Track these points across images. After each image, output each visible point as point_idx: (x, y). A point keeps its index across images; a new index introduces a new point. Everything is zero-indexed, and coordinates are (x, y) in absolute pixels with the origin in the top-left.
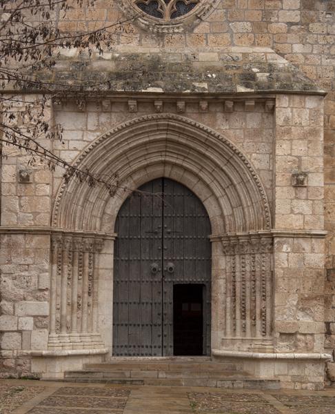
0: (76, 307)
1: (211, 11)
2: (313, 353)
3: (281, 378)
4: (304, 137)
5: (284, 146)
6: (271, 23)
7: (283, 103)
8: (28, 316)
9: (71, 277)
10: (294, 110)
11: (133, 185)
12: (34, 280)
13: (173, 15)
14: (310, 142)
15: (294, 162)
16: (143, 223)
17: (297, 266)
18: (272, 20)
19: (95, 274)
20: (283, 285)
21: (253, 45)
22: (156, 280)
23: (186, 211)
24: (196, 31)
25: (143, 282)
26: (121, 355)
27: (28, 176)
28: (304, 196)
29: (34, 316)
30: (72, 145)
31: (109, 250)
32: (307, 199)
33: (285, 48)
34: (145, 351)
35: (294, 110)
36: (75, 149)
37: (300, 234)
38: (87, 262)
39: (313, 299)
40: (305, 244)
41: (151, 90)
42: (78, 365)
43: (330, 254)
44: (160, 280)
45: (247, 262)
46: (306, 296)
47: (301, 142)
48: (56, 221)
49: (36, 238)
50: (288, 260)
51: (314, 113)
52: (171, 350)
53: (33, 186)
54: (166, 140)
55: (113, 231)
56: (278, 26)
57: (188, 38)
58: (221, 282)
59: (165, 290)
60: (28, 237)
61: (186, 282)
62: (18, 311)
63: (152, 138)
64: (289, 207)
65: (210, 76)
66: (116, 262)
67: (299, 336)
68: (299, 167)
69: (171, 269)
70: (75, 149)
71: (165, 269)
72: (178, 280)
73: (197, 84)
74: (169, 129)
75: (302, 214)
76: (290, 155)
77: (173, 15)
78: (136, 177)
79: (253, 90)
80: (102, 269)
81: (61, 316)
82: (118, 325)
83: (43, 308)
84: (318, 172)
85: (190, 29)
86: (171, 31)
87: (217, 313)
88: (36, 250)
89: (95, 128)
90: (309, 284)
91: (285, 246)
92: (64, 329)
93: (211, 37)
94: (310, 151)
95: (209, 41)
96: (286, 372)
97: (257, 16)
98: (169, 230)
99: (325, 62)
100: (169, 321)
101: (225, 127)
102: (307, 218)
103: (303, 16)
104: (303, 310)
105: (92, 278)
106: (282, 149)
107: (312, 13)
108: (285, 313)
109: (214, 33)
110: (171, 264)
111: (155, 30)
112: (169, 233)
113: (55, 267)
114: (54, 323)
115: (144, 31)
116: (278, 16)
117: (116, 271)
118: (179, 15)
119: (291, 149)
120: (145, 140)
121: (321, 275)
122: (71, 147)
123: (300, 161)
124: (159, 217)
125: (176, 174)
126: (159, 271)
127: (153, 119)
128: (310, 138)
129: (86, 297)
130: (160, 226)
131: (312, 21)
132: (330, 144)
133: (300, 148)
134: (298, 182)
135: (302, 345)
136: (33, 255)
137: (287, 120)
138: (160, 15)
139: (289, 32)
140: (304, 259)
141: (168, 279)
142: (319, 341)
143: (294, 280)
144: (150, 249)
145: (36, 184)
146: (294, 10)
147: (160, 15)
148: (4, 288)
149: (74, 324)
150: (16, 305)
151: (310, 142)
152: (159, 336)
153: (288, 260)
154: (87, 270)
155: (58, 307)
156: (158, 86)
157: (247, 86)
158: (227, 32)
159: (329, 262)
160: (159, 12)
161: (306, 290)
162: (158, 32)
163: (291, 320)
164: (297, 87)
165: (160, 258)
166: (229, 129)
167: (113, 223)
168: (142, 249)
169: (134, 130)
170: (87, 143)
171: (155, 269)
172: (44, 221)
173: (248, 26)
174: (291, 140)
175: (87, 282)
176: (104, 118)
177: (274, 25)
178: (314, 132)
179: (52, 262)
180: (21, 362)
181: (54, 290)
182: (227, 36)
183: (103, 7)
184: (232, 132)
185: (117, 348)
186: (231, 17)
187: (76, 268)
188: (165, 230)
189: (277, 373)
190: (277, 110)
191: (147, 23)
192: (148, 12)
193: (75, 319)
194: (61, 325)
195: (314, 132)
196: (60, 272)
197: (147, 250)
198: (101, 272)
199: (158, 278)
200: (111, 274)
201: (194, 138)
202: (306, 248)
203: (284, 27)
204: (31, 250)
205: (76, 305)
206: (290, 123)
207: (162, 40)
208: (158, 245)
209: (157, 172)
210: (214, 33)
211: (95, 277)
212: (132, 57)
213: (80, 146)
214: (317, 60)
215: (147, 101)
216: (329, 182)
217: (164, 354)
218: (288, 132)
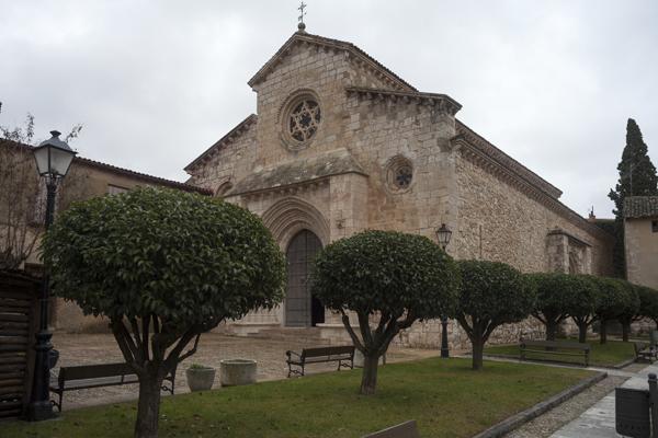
7: (333, 180)
33: (351, 146)
42: (256, 330)
78: (290, 230)
97: (338, 130)
100: (309, 307)
101: (313, 198)
106: (333, 207)
125: (307, 227)
131: (365, 126)
133: (341, 205)
137: (335, 191)
139: (355, 134)
164: (340, 170)
169: (277, 206)
173: (334, 137)
176: (265, 203)
178: (348, 195)
195: (348, 195)
201: (302, 206)
203: (351, 133)
215: (277, 191)
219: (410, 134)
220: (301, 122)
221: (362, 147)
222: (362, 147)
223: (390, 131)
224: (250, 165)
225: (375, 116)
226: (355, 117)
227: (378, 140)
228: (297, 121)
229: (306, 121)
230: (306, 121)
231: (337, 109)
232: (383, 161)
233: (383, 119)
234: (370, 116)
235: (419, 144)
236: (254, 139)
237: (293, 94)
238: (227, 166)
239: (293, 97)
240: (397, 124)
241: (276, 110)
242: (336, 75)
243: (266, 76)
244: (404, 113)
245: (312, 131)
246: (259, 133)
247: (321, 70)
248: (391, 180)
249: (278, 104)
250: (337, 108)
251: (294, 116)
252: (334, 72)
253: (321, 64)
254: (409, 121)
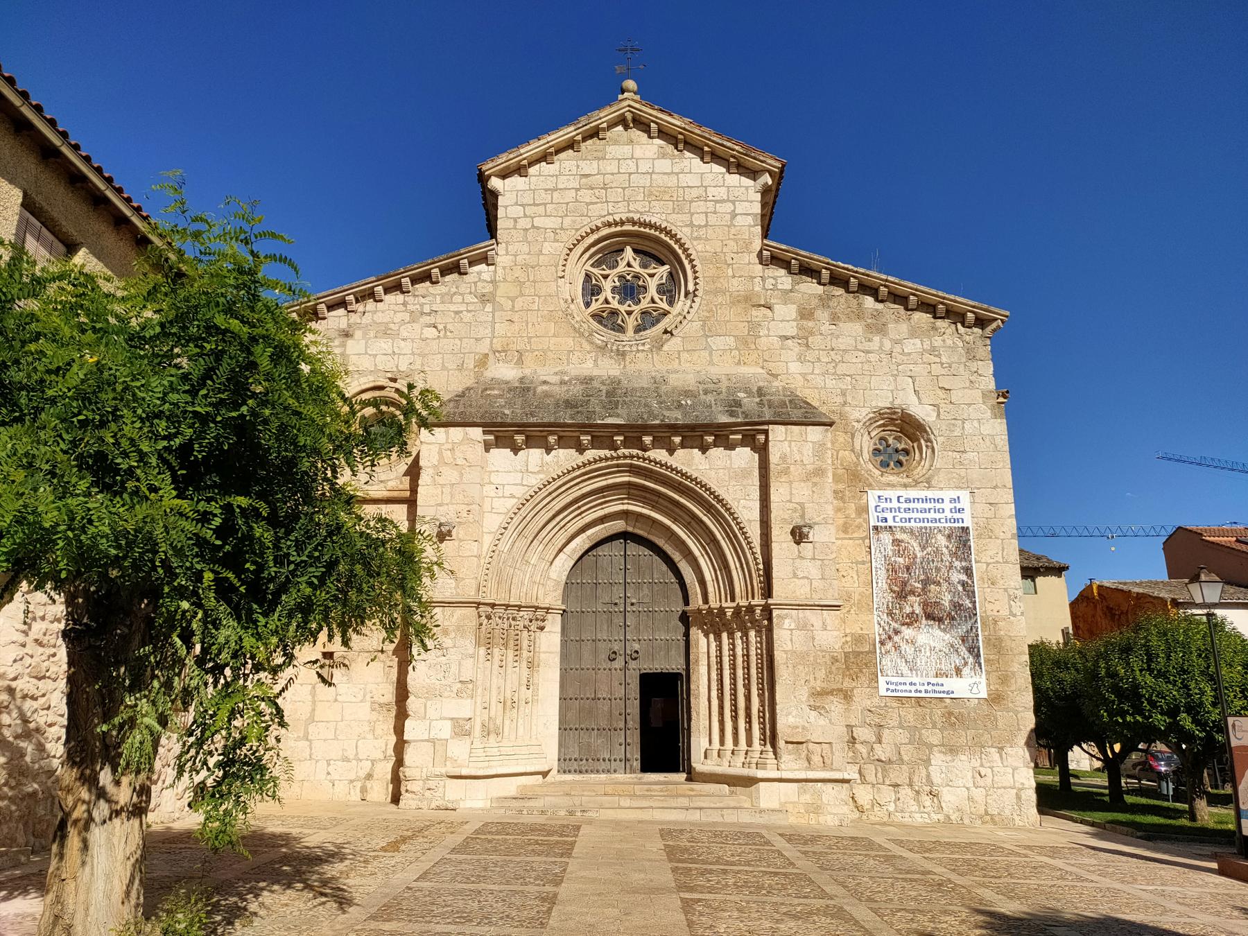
0: (510, 704)
1: (685, 322)
2: (832, 770)
3: (790, 807)
4: (807, 478)
5: (781, 490)
6: (760, 337)
8: (446, 719)
9: (504, 663)
10: (793, 443)
11: (587, 541)
12: (454, 668)
13: (638, 329)
14: (815, 484)
15: (795, 510)
16: (599, 591)
17: (806, 649)
18: (761, 334)
19: (536, 659)
20: (786, 675)
21: (739, 363)
23: (655, 576)
24: (665, 348)
26: (570, 772)
27: (450, 531)
28: (809, 554)
29: (452, 719)
30: (508, 490)
31: (554, 625)
32: (814, 559)
34: (603, 766)
35: (793, 443)
36: (512, 496)
37: (807, 605)
38: (525, 644)
39: (827, 694)
40: (813, 617)
41: (609, 421)
43: (848, 631)
45: (739, 642)
46: (819, 689)
47: (803, 484)
48: (484, 589)
49: (459, 612)
50: (791, 640)
51: (820, 449)
52: (637, 764)
53: (456, 543)
54: (629, 484)
55: (560, 602)
56: (768, 341)
57: (655, 355)
58: (703, 669)
59: (628, 680)
60: (448, 611)
62: (431, 713)
63: (610, 481)
64: (790, 569)
65: (683, 402)
66: (564, 643)
67: (811, 746)
68: (802, 516)
70: (512, 496)
71: (628, 652)
73: (667, 413)
74: (634, 470)
75: (808, 578)
76: (791, 502)
77: (638, 329)
79: (739, 420)
80: (544, 652)
81: (490, 718)
82: (565, 730)
83: (463, 709)
84: (826, 523)
85: (658, 345)
86: (634, 348)
87: (698, 714)
88: (459, 629)
89: (538, 469)
90: (821, 674)
91: (787, 621)
92: (492, 736)
93: (685, 356)
94: (815, 495)
95: (682, 361)
96: (796, 800)
97: (743, 329)
98: (634, 601)
99: (830, 383)
102: (815, 584)
103: (800, 328)
104: (813, 708)
105: (531, 665)
107: (811, 324)
108: (790, 714)
109: (688, 351)
110: (636, 646)
111: (614, 348)
112: (632, 604)
113: (482, 651)
114: (478, 728)
115: (603, 348)
116: (769, 330)
117: (565, 656)
118: (645, 329)
119: (791, 494)
120: (604, 483)
121: (837, 661)
122: (507, 494)
123: (803, 509)
127: (612, 458)
128: (815, 480)
129: (525, 694)
131: (812, 333)
132: (841, 486)
133: (802, 492)
134: (799, 535)
135: (816, 759)
136: (453, 635)
137: (783, 458)
138: (621, 329)
140: (814, 639)
142: (840, 754)
143: (801, 668)
145: (461, 540)
146: (788, 321)
147: (621, 329)
148: (414, 680)
149: (506, 730)
150: (429, 703)
151: (815, 484)
152: (620, 745)
153: (791, 640)
154: (525, 654)
155: (486, 705)
156: (618, 416)
157: (731, 416)
158: (705, 348)
159: (847, 642)
160: (619, 325)
161: (818, 682)
162: (618, 350)
163: (800, 722)
165: (622, 638)
166: (710, 469)
167: (560, 591)
170: (527, 488)
172: (470, 594)
174: (791, 483)
175: (525, 672)
177: (764, 340)
178: (819, 472)
179: (478, 644)
180: (431, 784)
181: (479, 683)
182: (706, 354)
183: (549, 320)
184: (713, 473)
185: (567, 763)
186: (708, 330)
187: (511, 653)
188: (628, 600)
189: (782, 800)
190: (770, 444)
191: (604, 339)
192: (605, 326)
193: (507, 722)
194: (489, 731)
195: (819, 472)
196: (489, 657)
197: (605, 628)
198: (542, 656)
199: (619, 663)
200: (557, 660)
202: (815, 624)
204: (451, 629)
205: (509, 703)
206: (789, 461)
207: (624, 359)
209: (618, 526)
210: (688, 351)
211: (536, 663)
212: (587, 380)
213: (521, 492)
214: (819, 381)
216: (843, 535)
217: (628, 770)
218: (786, 471)
219: (919, 369)
220: (614, 290)
221: (804, 375)
222: (804, 375)
223: (874, 358)
224: (470, 363)
225: (834, 319)
226: (790, 311)
227: (841, 369)
228: (607, 286)
229: (629, 290)
230: (629, 290)
231: (736, 285)
232: (859, 413)
233: (857, 328)
234: (823, 315)
235: (940, 392)
236: (484, 299)
237: (609, 225)
238: (384, 345)
239: (605, 231)
240: (887, 345)
241: (561, 248)
242: (734, 215)
243: (531, 164)
244: (904, 327)
245: (649, 319)
246: (502, 290)
247: (695, 193)
248: (866, 456)
249: (569, 237)
250: (735, 282)
251: (595, 271)
252: (728, 207)
253: (692, 180)
254: (914, 345)
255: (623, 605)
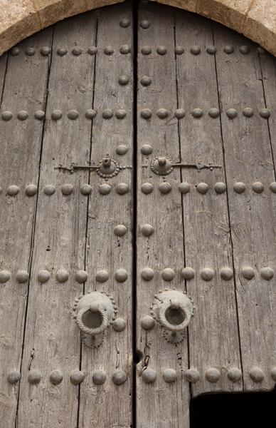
22: (101, 370)
23: (226, 99)
25: (35, 382)
44: (120, 373)
61: (256, 380)
69: (175, 313)
71: (145, 318)
72: (212, 370)
112: (162, 170)
124: (121, 117)
126: (118, 329)
130: (122, 147)
141: (160, 366)
144: (76, 238)
165: (123, 271)
168: (40, 234)
171: (94, 316)
197: (66, 237)
208: (114, 214)
255: (127, 175)
